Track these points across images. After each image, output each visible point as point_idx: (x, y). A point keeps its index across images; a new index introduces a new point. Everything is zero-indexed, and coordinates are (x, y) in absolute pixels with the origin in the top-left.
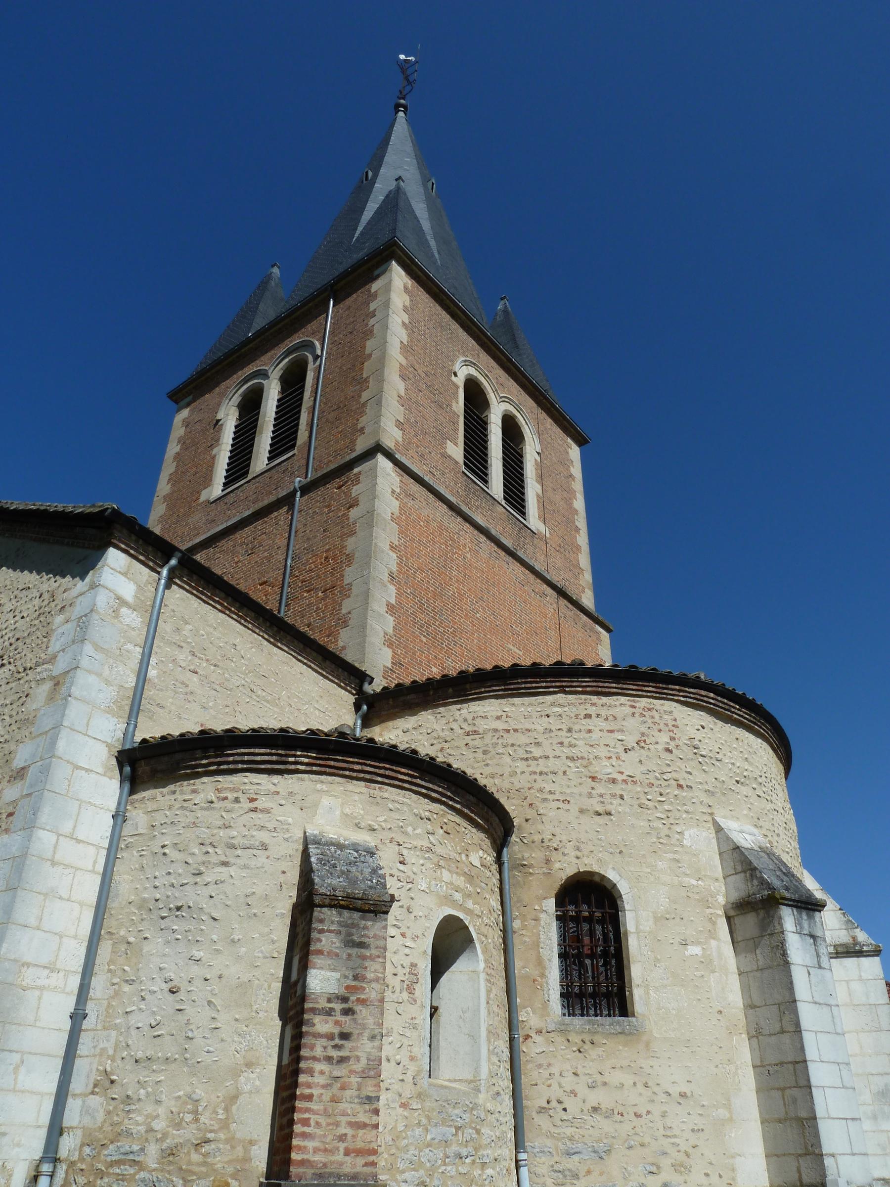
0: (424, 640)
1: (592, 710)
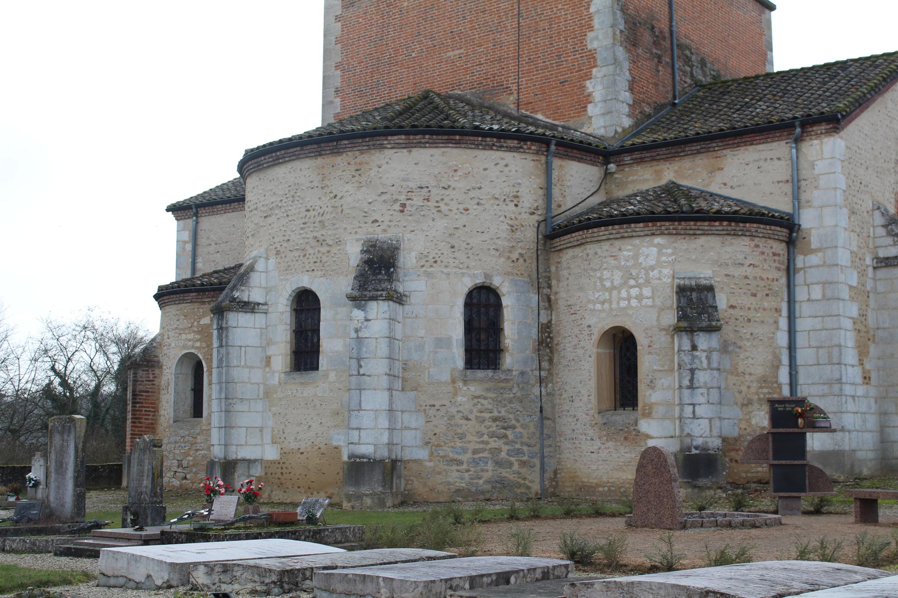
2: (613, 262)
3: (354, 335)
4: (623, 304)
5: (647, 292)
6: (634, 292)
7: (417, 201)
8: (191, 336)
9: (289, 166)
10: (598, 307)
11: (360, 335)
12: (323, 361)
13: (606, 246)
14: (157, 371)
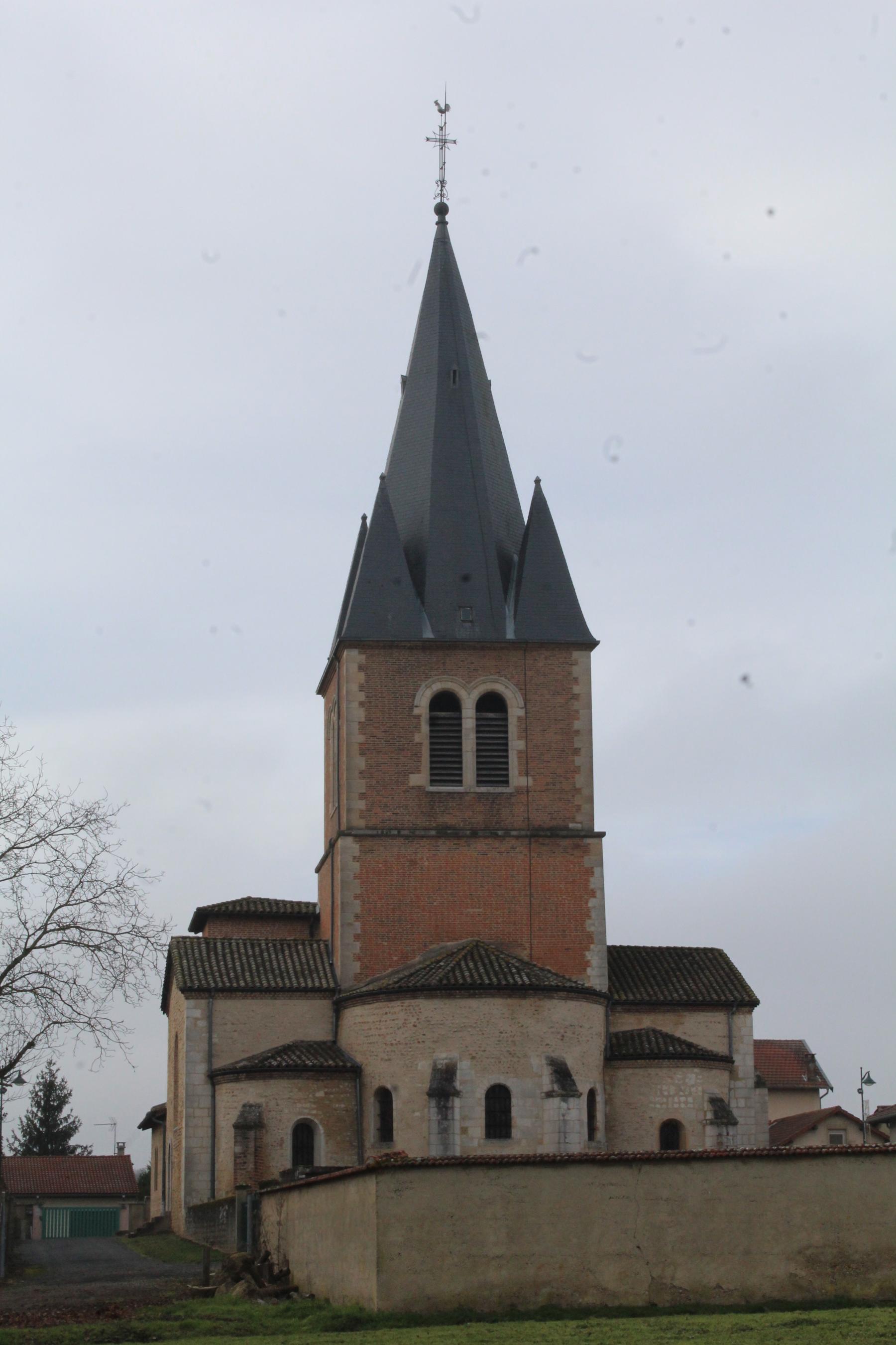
0: (386, 944)
1: (387, 1010)
2: (669, 1080)
3: (562, 1118)
4: (676, 1106)
5: (690, 1100)
6: (683, 1099)
7: (569, 1034)
8: (308, 1105)
9: (484, 1000)
10: (658, 1106)
11: (566, 1118)
12: (515, 1133)
13: (665, 1071)
14: (264, 1131)
